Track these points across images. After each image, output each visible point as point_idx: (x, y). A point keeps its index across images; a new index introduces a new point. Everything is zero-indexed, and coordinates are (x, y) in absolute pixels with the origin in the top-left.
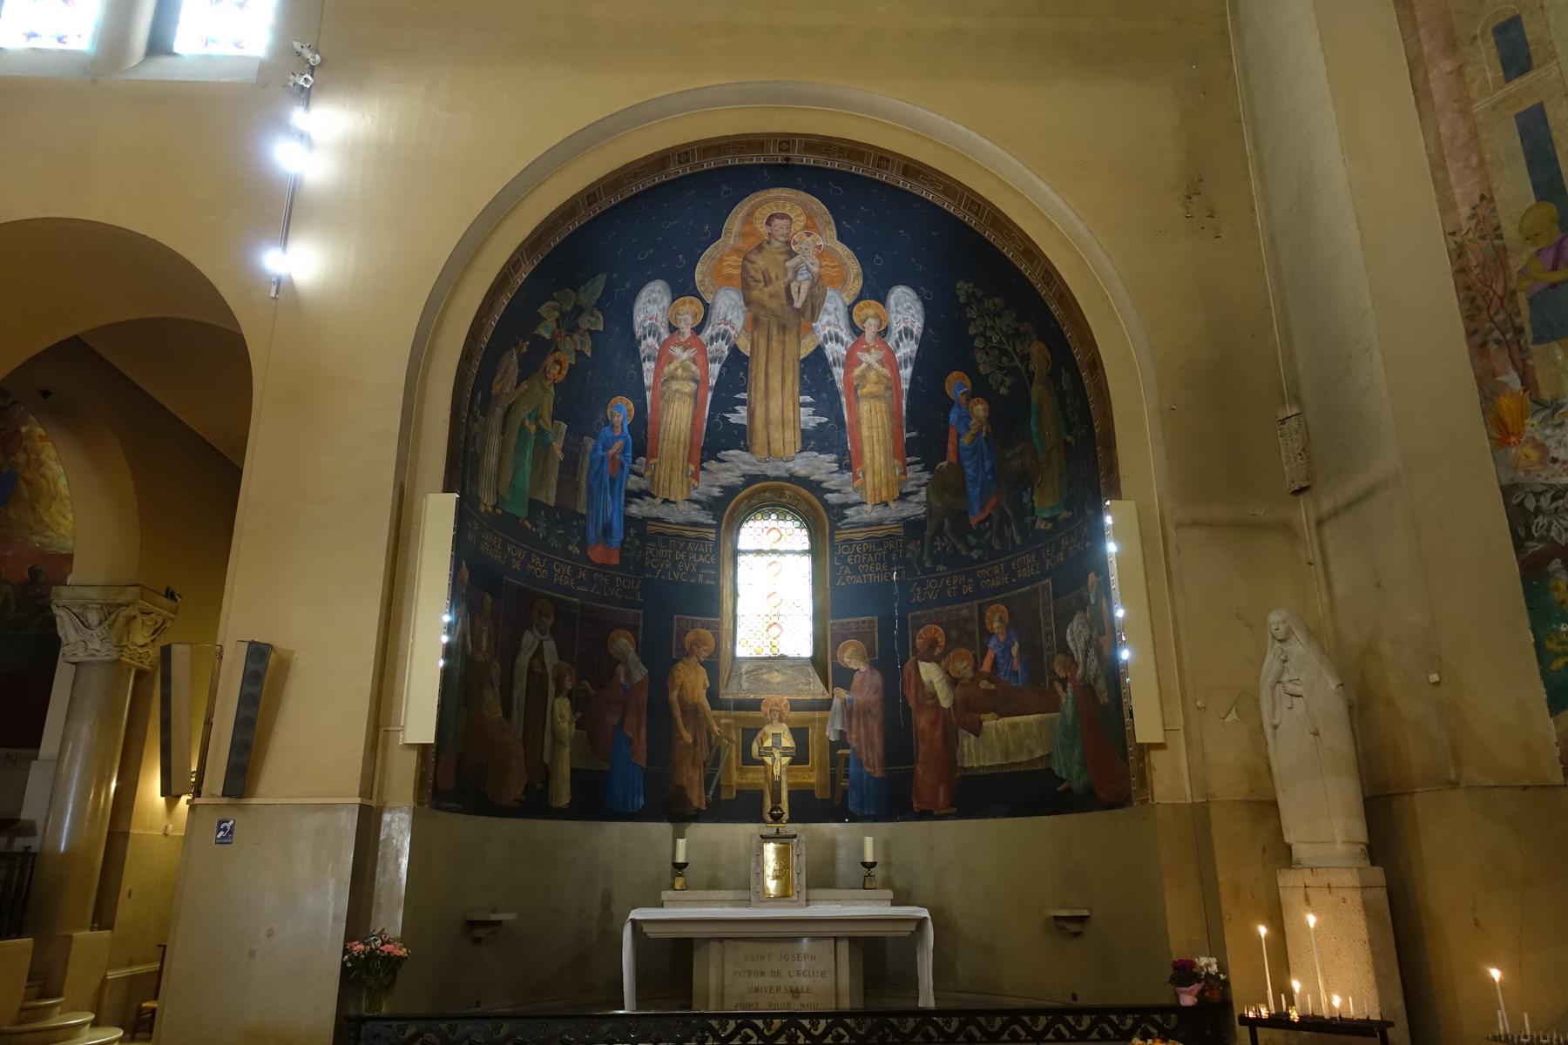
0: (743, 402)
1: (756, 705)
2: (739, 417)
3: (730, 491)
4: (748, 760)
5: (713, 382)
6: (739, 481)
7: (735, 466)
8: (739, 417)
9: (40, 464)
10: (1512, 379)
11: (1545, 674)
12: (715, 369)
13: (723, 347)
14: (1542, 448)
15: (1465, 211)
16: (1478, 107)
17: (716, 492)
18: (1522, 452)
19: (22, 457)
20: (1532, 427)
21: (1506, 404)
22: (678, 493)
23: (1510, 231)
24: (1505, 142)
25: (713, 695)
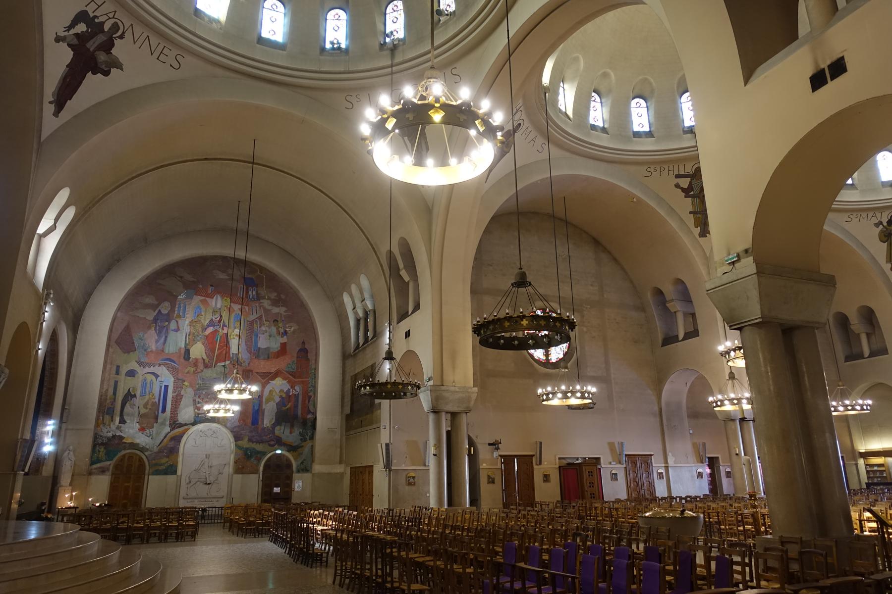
10: (101, 418)
11: (91, 460)
14: (102, 430)
15: (104, 391)
16: (111, 375)
18: (99, 429)
20: (101, 426)
21: (99, 422)
23: (108, 397)
24: (112, 383)
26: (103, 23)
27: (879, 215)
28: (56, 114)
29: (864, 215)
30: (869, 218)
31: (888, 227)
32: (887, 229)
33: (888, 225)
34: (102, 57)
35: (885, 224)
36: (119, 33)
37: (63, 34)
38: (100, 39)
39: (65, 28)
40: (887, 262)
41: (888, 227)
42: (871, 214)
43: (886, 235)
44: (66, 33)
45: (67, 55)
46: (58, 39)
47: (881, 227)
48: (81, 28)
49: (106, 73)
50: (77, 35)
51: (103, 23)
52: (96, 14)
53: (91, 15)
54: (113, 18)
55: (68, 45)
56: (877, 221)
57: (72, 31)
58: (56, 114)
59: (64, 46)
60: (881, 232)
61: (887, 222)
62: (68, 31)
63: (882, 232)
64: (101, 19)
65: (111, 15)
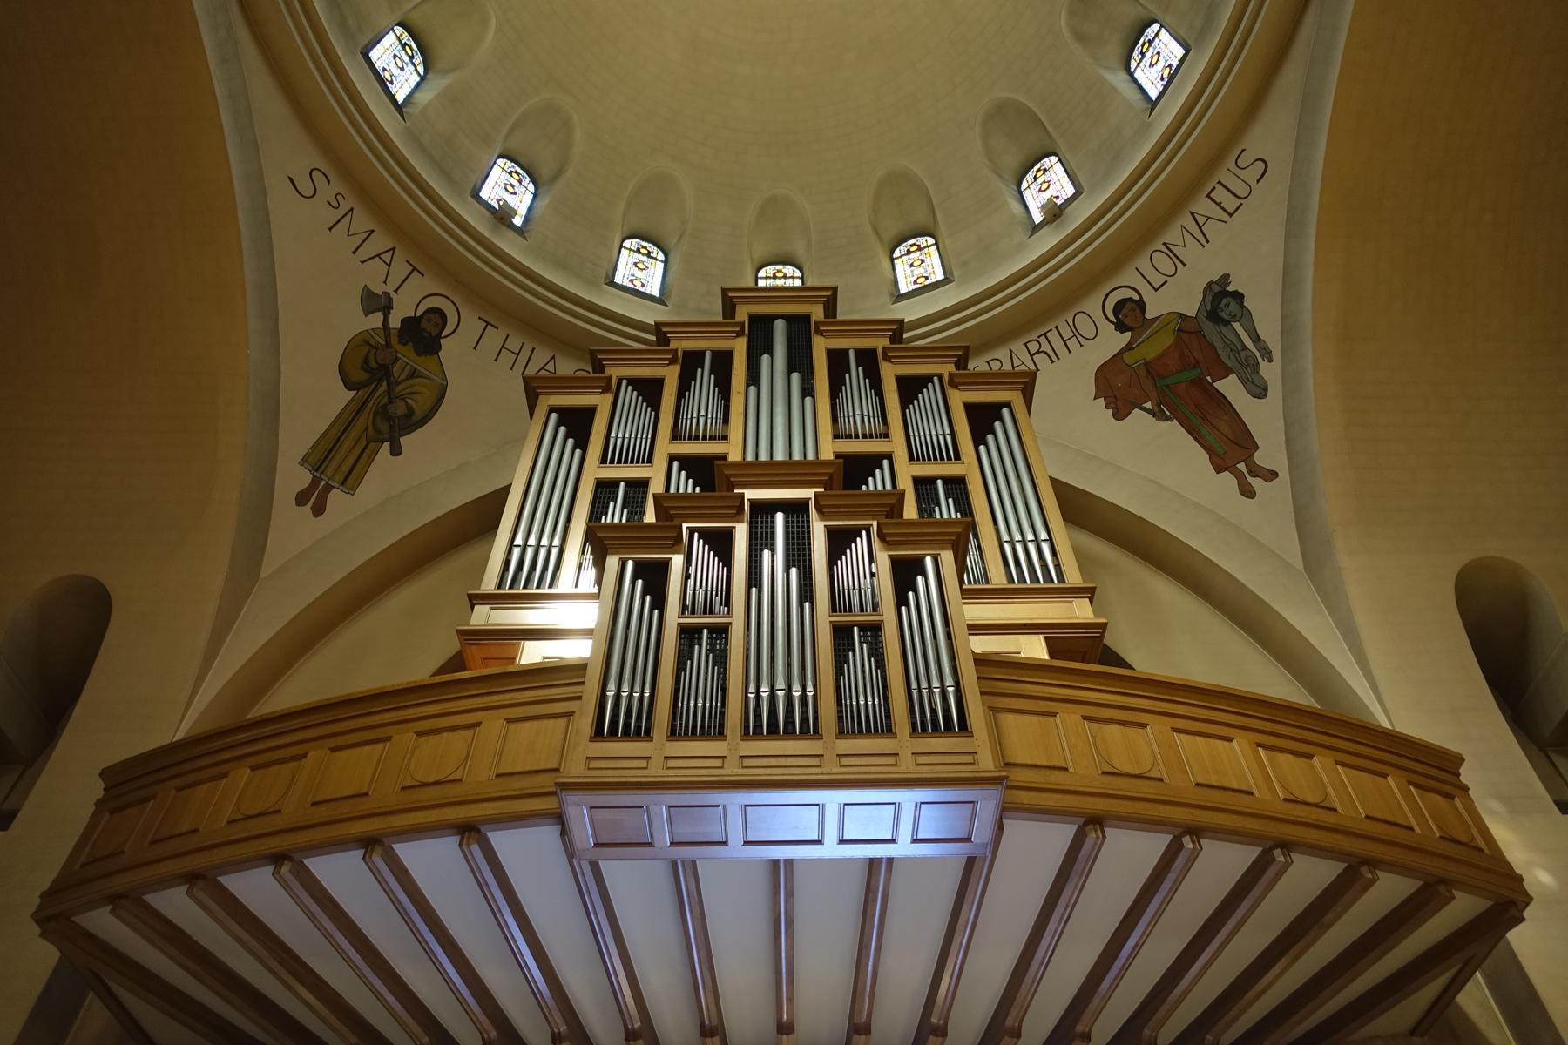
27: (400, 268)
29: (362, 221)
30: (367, 250)
31: (394, 340)
32: (388, 345)
33: (400, 331)
35: (395, 323)
40: (304, 461)
41: (394, 340)
42: (380, 242)
43: (374, 365)
47: (376, 320)
56: (378, 289)
60: (362, 342)
61: (403, 321)
63: (368, 343)
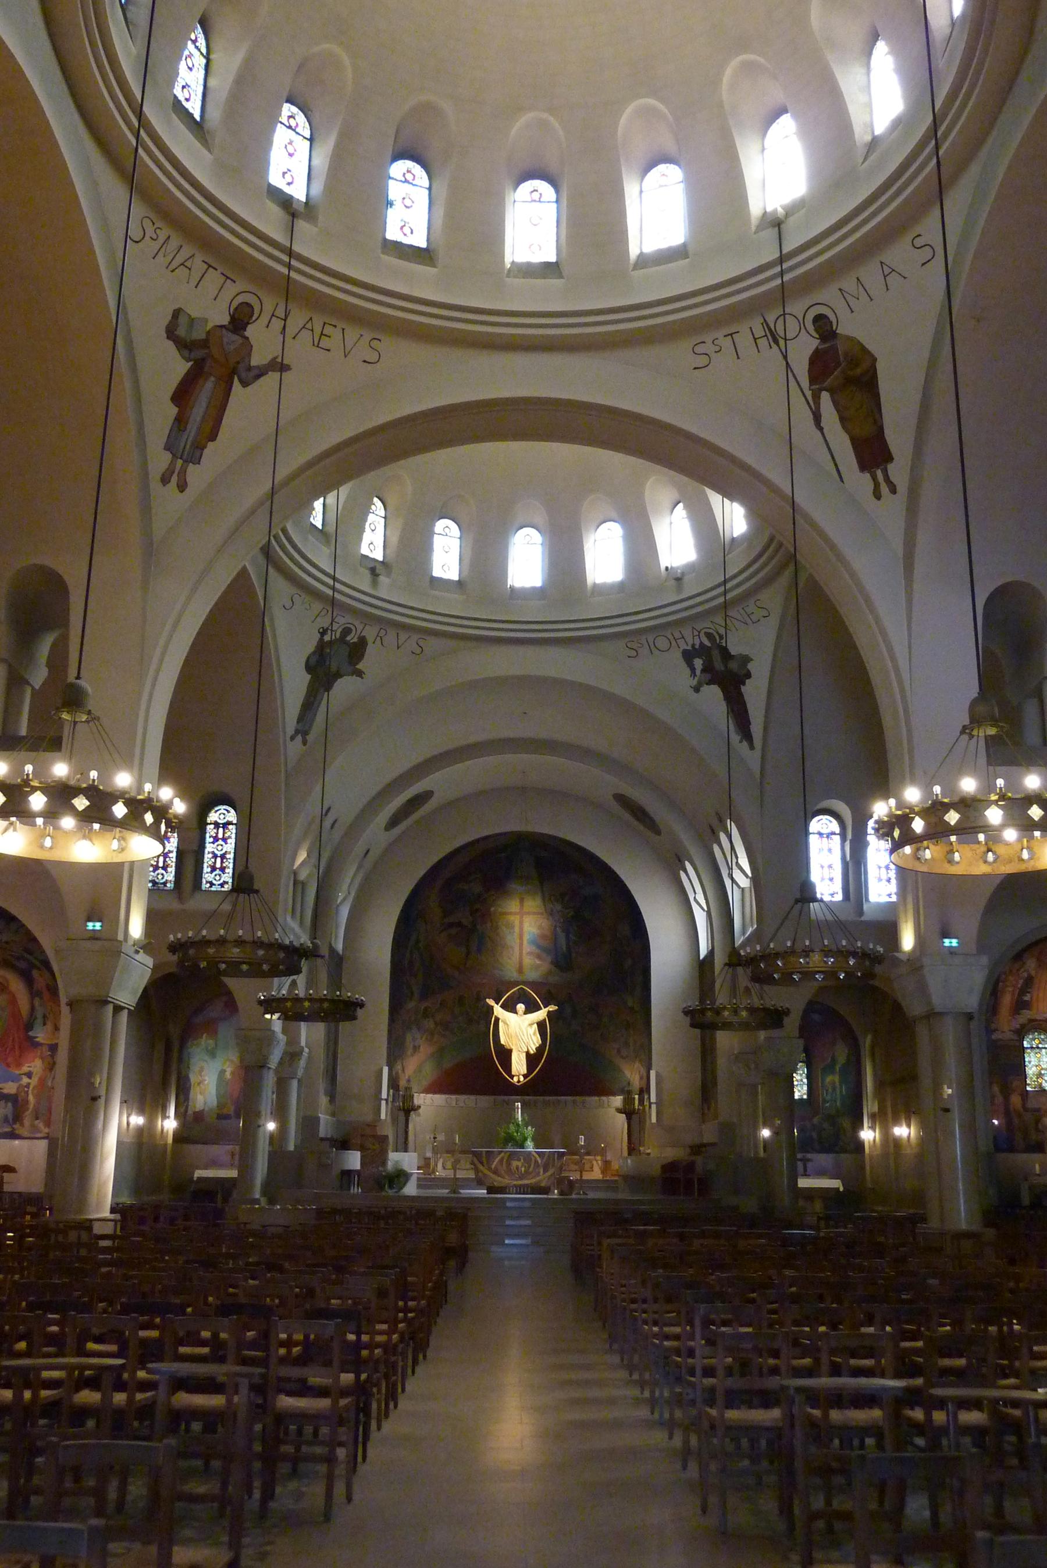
0: (1029, 992)
1: (1038, 1110)
2: (1027, 998)
3: (1023, 1026)
4: (1037, 1130)
5: (1019, 986)
6: (1026, 1022)
7: (1026, 1015)
8: (1027, 998)
9: (497, 928)
12: (1021, 982)
13: (1025, 975)
17: (1018, 1026)
19: (489, 925)
22: (1006, 1028)
25: (1024, 1106)
26: (701, 643)
28: (752, 747)
34: (733, 665)
36: (717, 637)
37: (695, 682)
38: (716, 654)
39: (691, 676)
44: (696, 679)
45: (714, 693)
46: (697, 689)
48: (698, 663)
49: (748, 675)
50: (703, 671)
51: (701, 643)
52: (690, 642)
53: (689, 648)
54: (699, 632)
55: (707, 684)
57: (698, 672)
58: (752, 747)
59: (705, 689)
62: (695, 675)
64: (697, 642)
65: (696, 633)
